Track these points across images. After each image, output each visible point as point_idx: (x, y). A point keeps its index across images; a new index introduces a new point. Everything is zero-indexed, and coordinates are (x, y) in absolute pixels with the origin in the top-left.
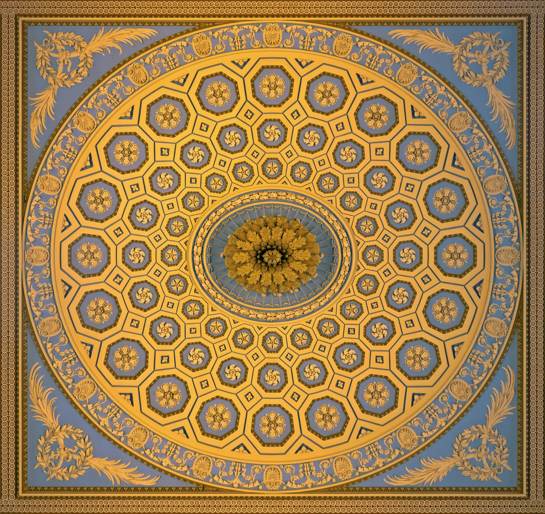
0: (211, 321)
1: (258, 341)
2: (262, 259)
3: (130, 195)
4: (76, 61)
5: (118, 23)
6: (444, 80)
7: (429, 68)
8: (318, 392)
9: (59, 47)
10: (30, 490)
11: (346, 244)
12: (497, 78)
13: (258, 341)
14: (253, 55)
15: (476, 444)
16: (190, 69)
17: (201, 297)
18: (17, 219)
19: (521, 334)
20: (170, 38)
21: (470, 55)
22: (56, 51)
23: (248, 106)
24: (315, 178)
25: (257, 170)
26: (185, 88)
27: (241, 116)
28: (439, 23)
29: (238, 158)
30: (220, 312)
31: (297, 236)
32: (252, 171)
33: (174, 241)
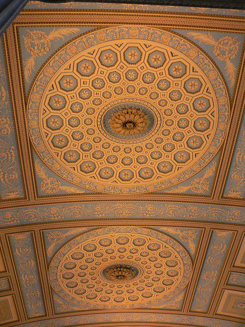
0: (104, 143)
1: (122, 150)
2: (126, 126)
4: (43, 44)
5: (62, 26)
6: (209, 57)
7: (203, 51)
9: (35, 38)
11: (159, 119)
12: (232, 58)
13: (122, 150)
14: (125, 42)
15: (198, 183)
16: (96, 48)
18: (23, 111)
19: (222, 152)
20: (87, 33)
21: (222, 46)
22: (33, 40)
23: (122, 64)
24: (148, 94)
26: (94, 56)
27: (119, 68)
28: (210, 31)
29: (116, 85)
30: (107, 141)
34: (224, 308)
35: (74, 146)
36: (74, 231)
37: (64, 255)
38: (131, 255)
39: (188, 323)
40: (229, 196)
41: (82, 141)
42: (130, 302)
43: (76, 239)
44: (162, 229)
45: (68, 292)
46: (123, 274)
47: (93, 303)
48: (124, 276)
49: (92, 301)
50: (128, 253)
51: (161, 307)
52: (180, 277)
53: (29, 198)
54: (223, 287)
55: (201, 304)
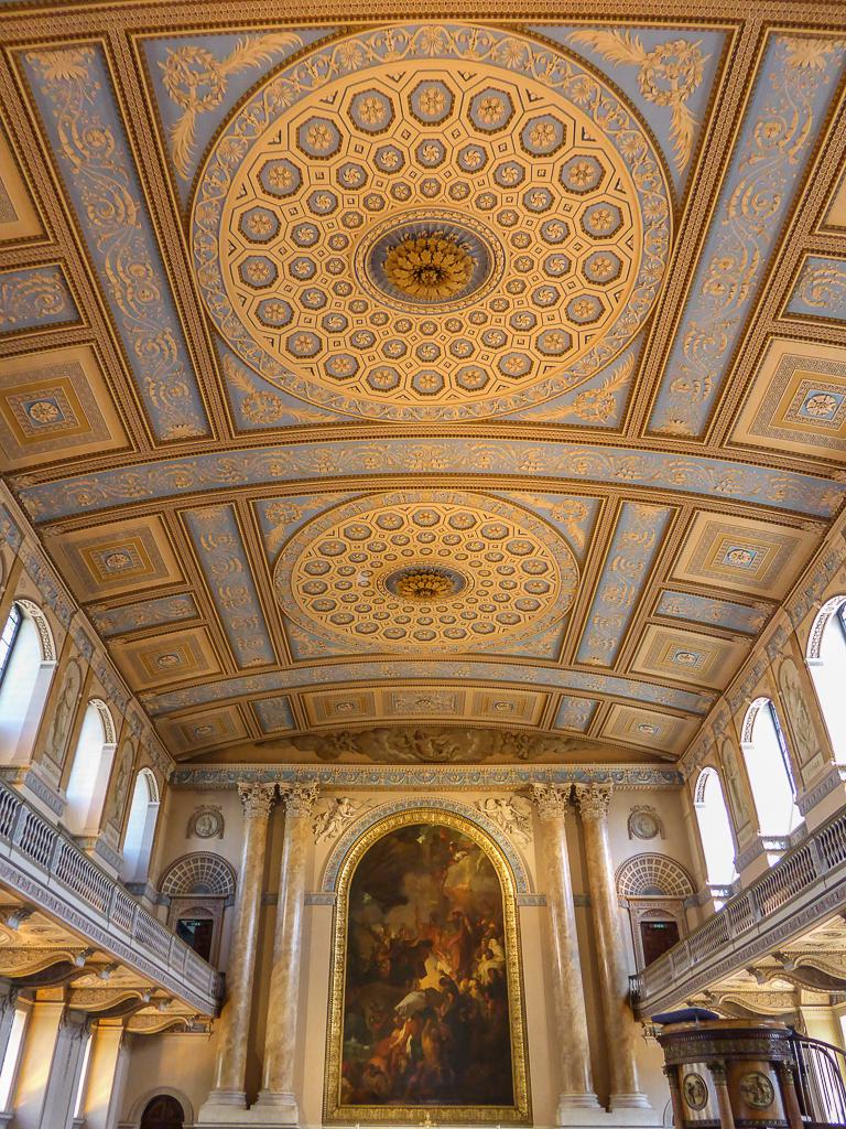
34: (763, 416)
37: (234, 172)
39: (637, 479)
42: (465, 397)
43: (267, 89)
45: (266, 345)
46: (437, 261)
47: (354, 396)
49: (342, 389)
51: (559, 415)
55: (682, 408)
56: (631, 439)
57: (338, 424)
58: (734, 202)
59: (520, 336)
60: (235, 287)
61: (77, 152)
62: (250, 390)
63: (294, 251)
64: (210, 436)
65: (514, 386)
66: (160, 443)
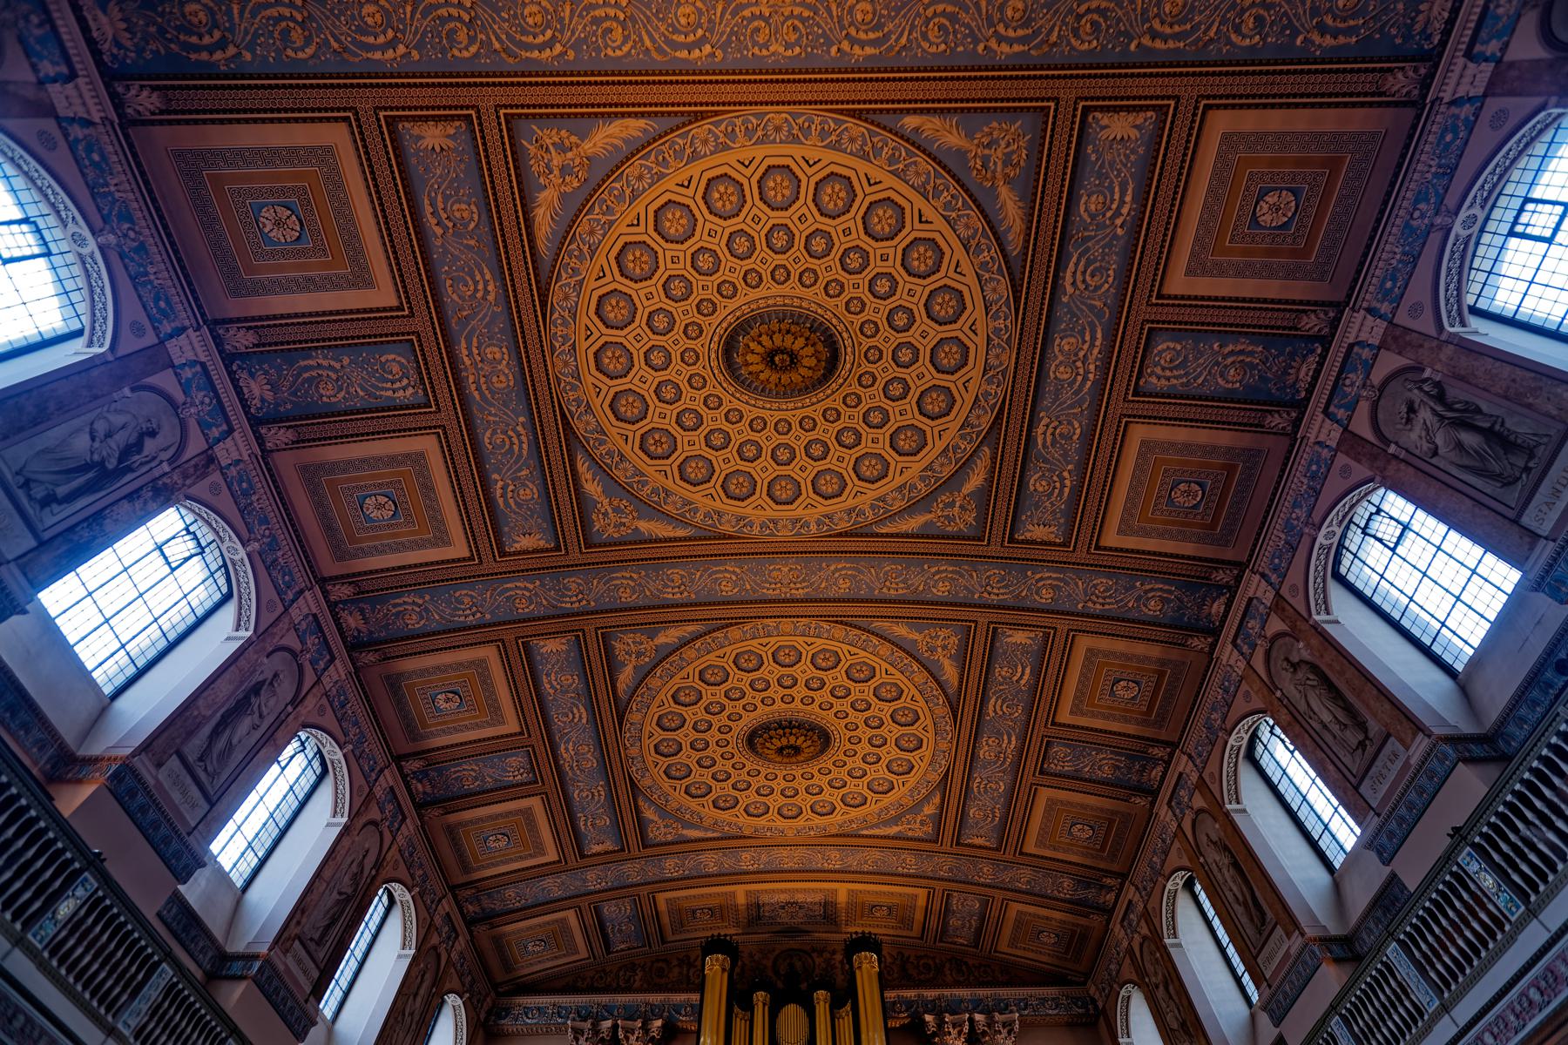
2: (773, 361)
3: (646, 303)
8: (821, 465)
10: (590, 547)
17: (719, 391)
25: (766, 277)
31: (807, 345)
32: (761, 278)
33: (691, 344)
35: (661, 416)
36: (669, 636)
38: (811, 693)
40: (1028, 535)
41: (679, 406)
44: (877, 624)
48: (797, 750)
49: (725, 815)
50: (800, 691)
52: (927, 752)
53: (566, 549)
54: (1031, 780)
56: (947, 847)
57: (722, 839)
58: (991, 707)
59: (856, 781)
60: (651, 757)
61: (552, 687)
62: (656, 819)
63: (694, 735)
64: (623, 850)
65: (854, 813)
66: (583, 856)
